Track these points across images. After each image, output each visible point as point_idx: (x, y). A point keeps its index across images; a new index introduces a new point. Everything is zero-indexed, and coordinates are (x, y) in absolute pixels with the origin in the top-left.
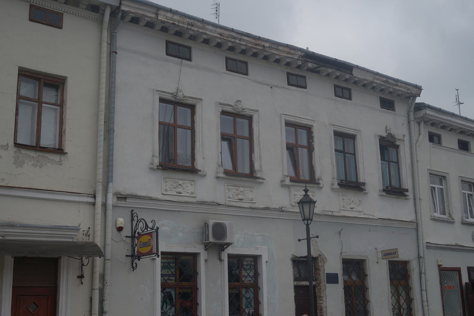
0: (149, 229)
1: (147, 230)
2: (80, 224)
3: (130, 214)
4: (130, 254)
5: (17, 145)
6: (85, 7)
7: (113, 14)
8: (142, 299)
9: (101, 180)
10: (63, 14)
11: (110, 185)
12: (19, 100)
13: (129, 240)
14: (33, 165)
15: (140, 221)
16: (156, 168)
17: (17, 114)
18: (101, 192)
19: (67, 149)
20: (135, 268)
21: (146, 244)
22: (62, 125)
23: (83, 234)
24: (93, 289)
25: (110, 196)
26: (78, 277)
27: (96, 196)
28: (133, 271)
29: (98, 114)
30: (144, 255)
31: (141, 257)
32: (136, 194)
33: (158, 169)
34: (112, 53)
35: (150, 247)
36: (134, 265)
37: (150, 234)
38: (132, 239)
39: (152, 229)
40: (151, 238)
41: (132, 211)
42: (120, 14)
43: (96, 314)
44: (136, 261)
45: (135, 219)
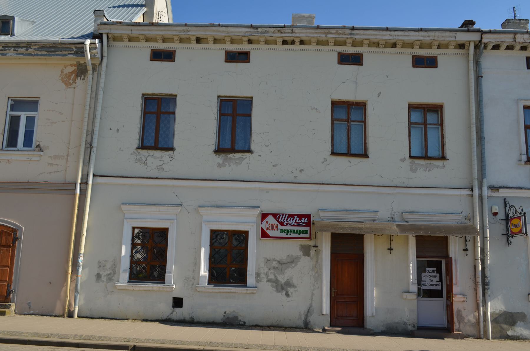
0: (518, 214)
1: (517, 215)
2: (462, 211)
3: (503, 201)
4: (505, 233)
5: (411, 157)
6: (453, 47)
7: (476, 47)
8: (518, 268)
9: (477, 177)
10: (437, 56)
11: (485, 180)
12: (410, 126)
13: (504, 222)
14: (424, 170)
15: (511, 208)
16: (524, 163)
17: (410, 136)
18: (477, 186)
19: (448, 157)
20: (510, 244)
21: (516, 226)
22: (443, 139)
23: (465, 218)
24: (476, 260)
25: (485, 189)
26: (464, 250)
27: (474, 189)
28: (509, 246)
29: (470, 126)
30: (516, 234)
31: (514, 236)
32: (508, 186)
33: (527, 164)
34: (479, 77)
35: (520, 228)
36: (509, 242)
37: (519, 218)
38: (506, 221)
39: (521, 213)
40: (520, 221)
41: (505, 199)
42: (483, 46)
43: (479, 278)
44: (510, 238)
45: (508, 205)
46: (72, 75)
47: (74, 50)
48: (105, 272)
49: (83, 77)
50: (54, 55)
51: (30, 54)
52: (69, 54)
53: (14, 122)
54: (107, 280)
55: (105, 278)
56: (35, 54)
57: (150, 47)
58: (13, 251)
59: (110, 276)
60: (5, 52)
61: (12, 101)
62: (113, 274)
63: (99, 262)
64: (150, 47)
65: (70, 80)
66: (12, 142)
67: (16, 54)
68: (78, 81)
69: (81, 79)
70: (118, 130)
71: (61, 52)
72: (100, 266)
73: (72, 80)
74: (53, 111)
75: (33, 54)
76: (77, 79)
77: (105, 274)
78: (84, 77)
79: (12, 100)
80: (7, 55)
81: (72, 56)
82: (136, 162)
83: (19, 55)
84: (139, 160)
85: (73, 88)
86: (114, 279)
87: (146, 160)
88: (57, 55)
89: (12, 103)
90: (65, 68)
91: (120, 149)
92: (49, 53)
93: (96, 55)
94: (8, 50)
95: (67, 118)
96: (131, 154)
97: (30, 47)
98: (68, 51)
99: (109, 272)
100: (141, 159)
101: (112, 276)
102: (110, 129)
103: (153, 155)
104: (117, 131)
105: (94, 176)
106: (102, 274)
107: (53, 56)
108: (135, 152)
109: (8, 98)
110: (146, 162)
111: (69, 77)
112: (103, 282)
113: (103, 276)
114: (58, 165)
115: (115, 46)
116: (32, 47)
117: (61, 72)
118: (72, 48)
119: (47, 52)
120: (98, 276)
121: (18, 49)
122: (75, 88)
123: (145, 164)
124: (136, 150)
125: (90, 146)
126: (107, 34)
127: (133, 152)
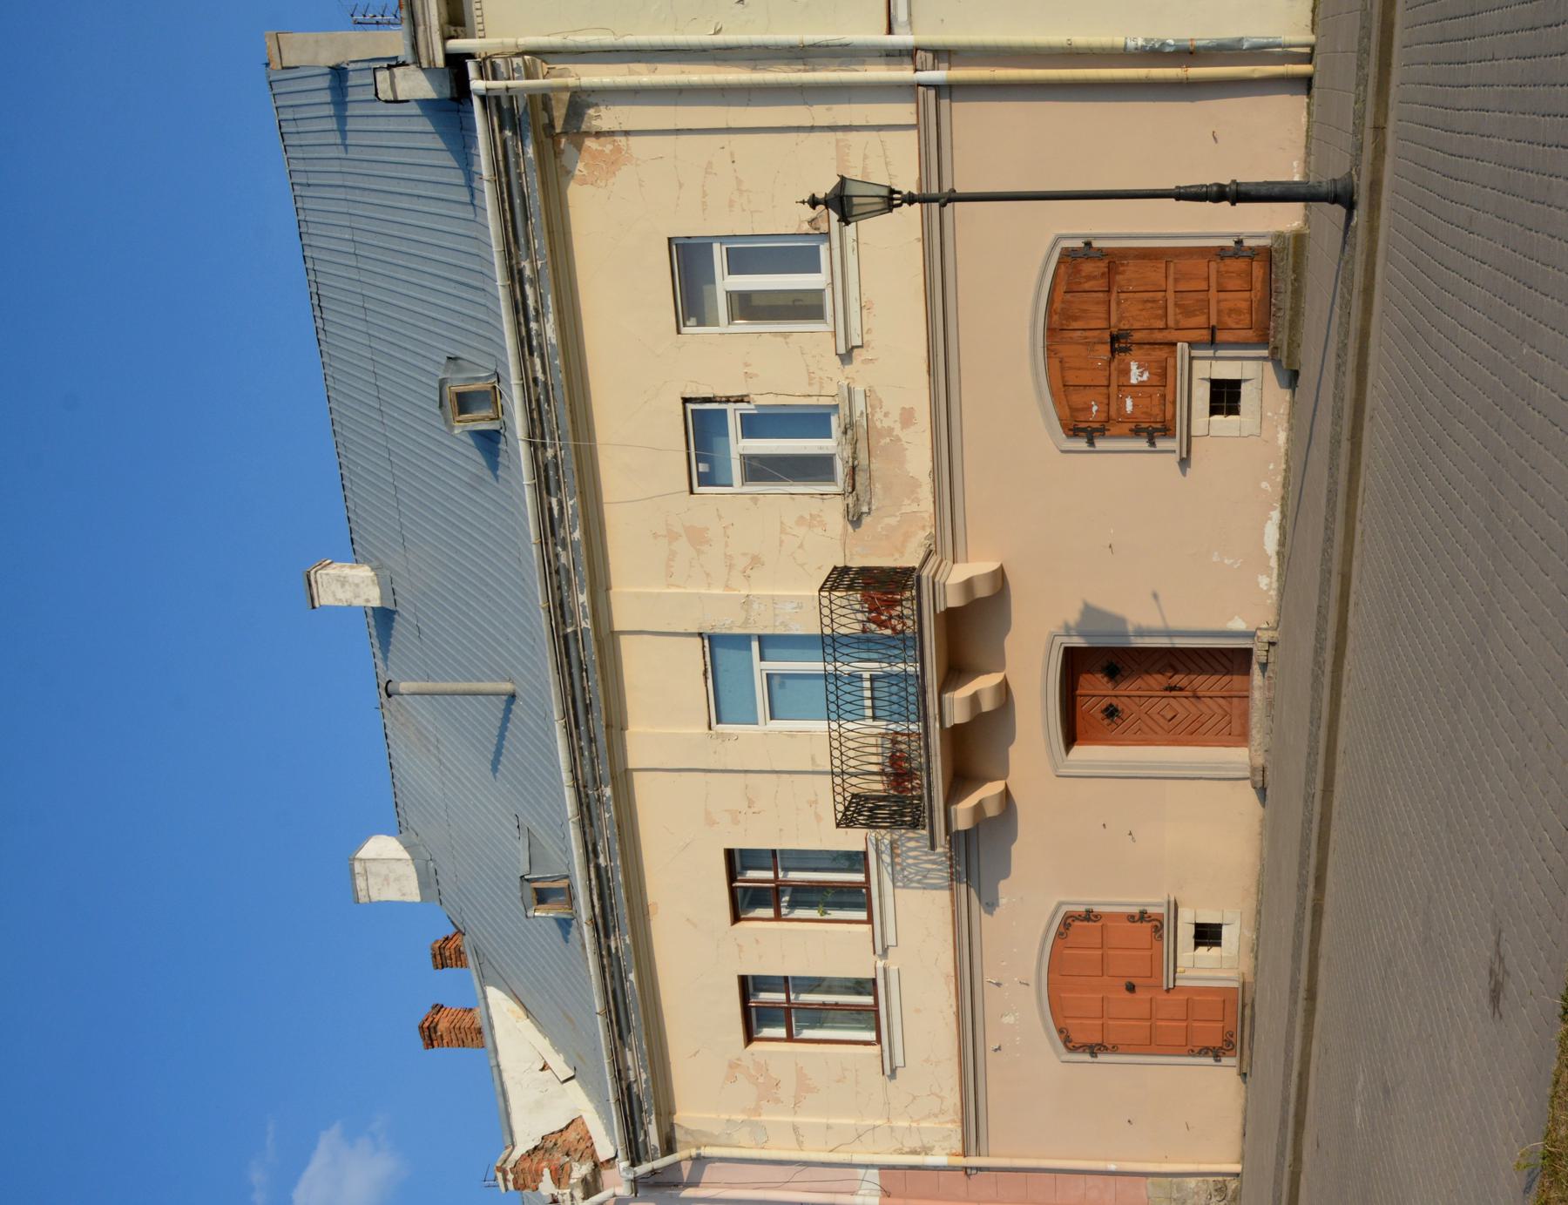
58: (1124, 254)
61: (688, 323)
66: (805, 307)
74: (705, 194)
79: (685, 325)
89: (695, 324)
114: (865, 157)
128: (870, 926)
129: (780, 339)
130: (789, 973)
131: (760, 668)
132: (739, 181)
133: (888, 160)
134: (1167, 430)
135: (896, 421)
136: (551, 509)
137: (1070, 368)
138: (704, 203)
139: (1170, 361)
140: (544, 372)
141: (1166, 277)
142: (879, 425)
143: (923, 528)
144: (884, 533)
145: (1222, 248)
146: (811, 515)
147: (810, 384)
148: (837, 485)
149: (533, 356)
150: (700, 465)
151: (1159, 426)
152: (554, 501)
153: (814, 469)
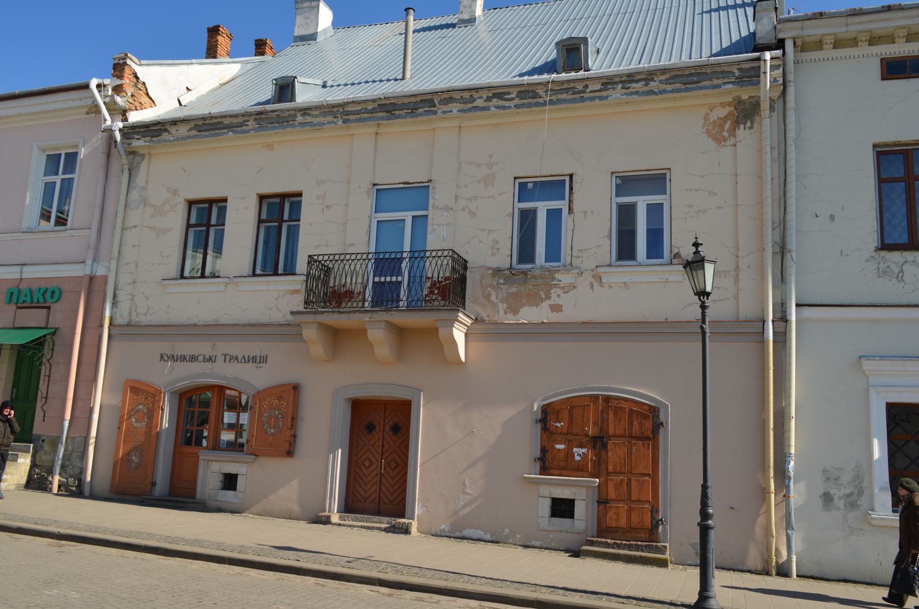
46: (725, 122)
47: (736, 75)
48: (839, 490)
49: (749, 124)
50: (695, 89)
51: (651, 92)
52: (725, 84)
53: (626, 214)
54: (845, 506)
55: (842, 502)
56: (659, 91)
57: (879, 54)
58: (656, 448)
59: (851, 499)
60: (604, 94)
61: (618, 179)
62: (858, 495)
63: (825, 471)
64: (879, 54)
65: (724, 131)
67: (626, 94)
68: (741, 132)
69: (745, 129)
70: (832, 217)
71: (710, 82)
72: (828, 479)
73: (727, 132)
74: (697, 190)
75: (657, 91)
76: (738, 129)
77: (841, 495)
78: (752, 123)
79: (616, 177)
80: (610, 98)
81: (730, 86)
82: (879, 277)
83: (630, 96)
84: (884, 272)
85: (731, 146)
86: (860, 505)
87: (902, 271)
88: (701, 88)
89: (617, 183)
90: (711, 111)
91: (842, 252)
92: (687, 86)
93: (777, 79)
94: (611, 88)
95: (726, 202)
96: (867, 261)
97: (652, 80)
98: (724, 78)
99: (848, 491)
100: (888, 270)
101: (856, 498)
102: (817, 216)
103: (914, 261)
104: (830, 218)
105: (797, 305)
106: (835, 494)
107: (695, 90)
108: (873, 257)
109: (610, 174)
110: (900, 275)
111: (721, 126)
112: (838, 509)
113: (836, 498)
115: (804, 61)
116: (655, 79)
117: (704, 120)
118: (732, 72)
119: (682, 85)
120: (827, 499)
121: (630, 85)
122: (735, 145)
123: (899, 278)
124: (875, 253)
125: (782, 250)
126: (794, 38)
127: (871, 256)
128: (251, 275)
129: (607, 233)
130: (226, 227)
131: (408, 216)
132: (704, 211)
133: (716, 302)
134: (544, 470)
135: (554, 301)
136: (509, 93)
137: (584, 411)
138: (691, 190)
139: (587, 474)
140: (591, 92)
141: (641, 474)
142: (553, 291)
143: (488, 316)
144: (486, 292)
145: (657, 511)
146: (499, 249)
147: (579, 250)
148: (517, 265)
149: (602, 85)
150: (532, 184)
151: (546, 464)
152: (514, 96)
153: (526, 251)
